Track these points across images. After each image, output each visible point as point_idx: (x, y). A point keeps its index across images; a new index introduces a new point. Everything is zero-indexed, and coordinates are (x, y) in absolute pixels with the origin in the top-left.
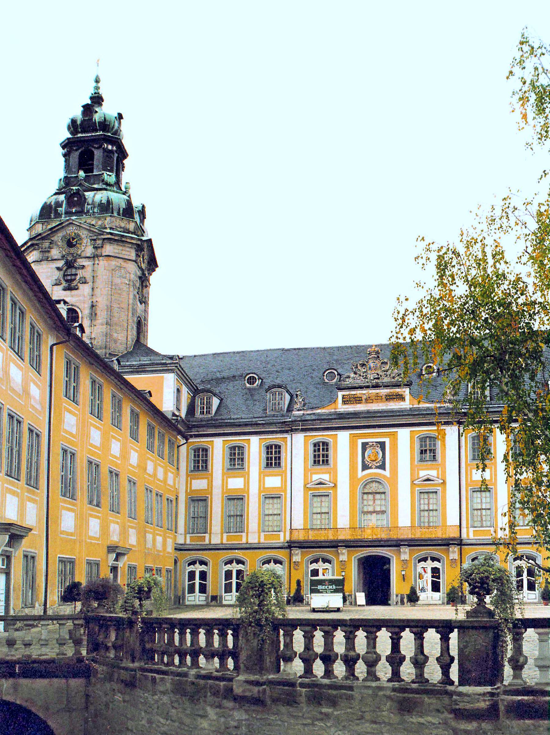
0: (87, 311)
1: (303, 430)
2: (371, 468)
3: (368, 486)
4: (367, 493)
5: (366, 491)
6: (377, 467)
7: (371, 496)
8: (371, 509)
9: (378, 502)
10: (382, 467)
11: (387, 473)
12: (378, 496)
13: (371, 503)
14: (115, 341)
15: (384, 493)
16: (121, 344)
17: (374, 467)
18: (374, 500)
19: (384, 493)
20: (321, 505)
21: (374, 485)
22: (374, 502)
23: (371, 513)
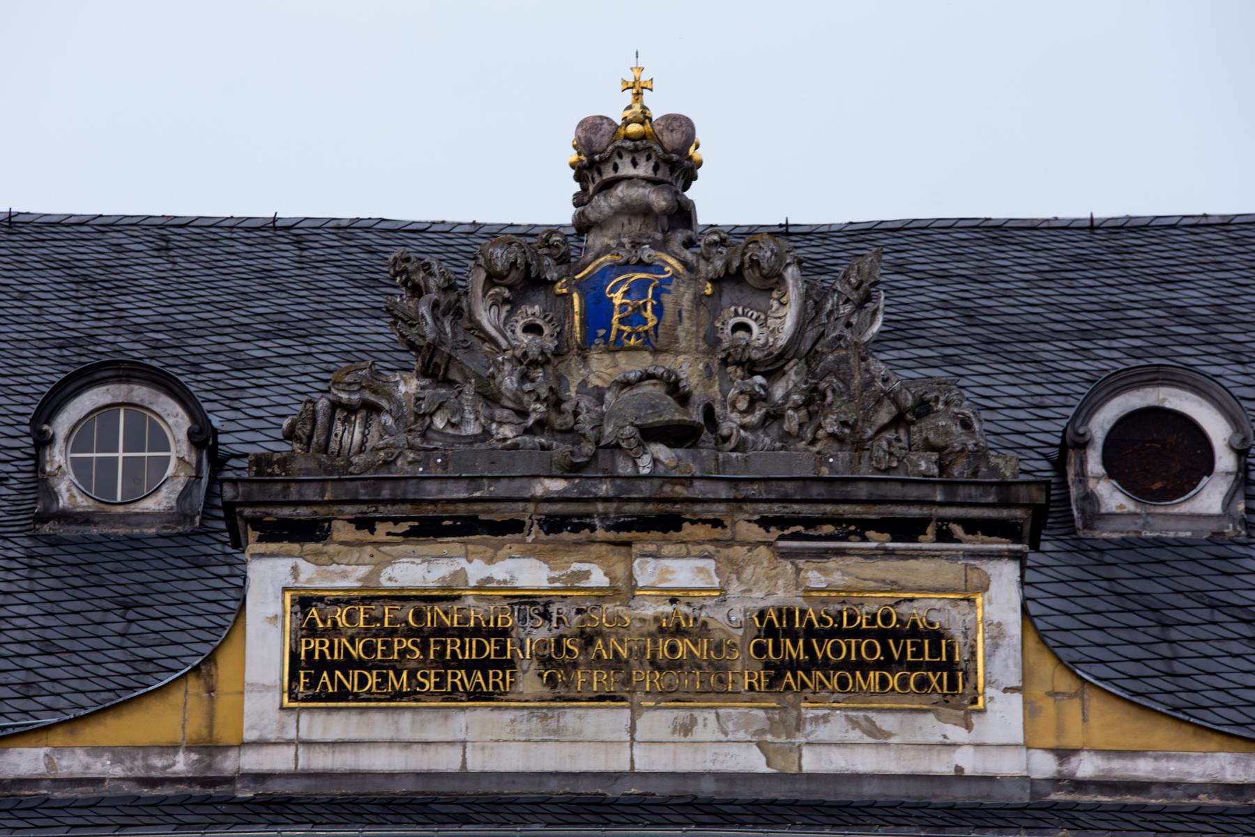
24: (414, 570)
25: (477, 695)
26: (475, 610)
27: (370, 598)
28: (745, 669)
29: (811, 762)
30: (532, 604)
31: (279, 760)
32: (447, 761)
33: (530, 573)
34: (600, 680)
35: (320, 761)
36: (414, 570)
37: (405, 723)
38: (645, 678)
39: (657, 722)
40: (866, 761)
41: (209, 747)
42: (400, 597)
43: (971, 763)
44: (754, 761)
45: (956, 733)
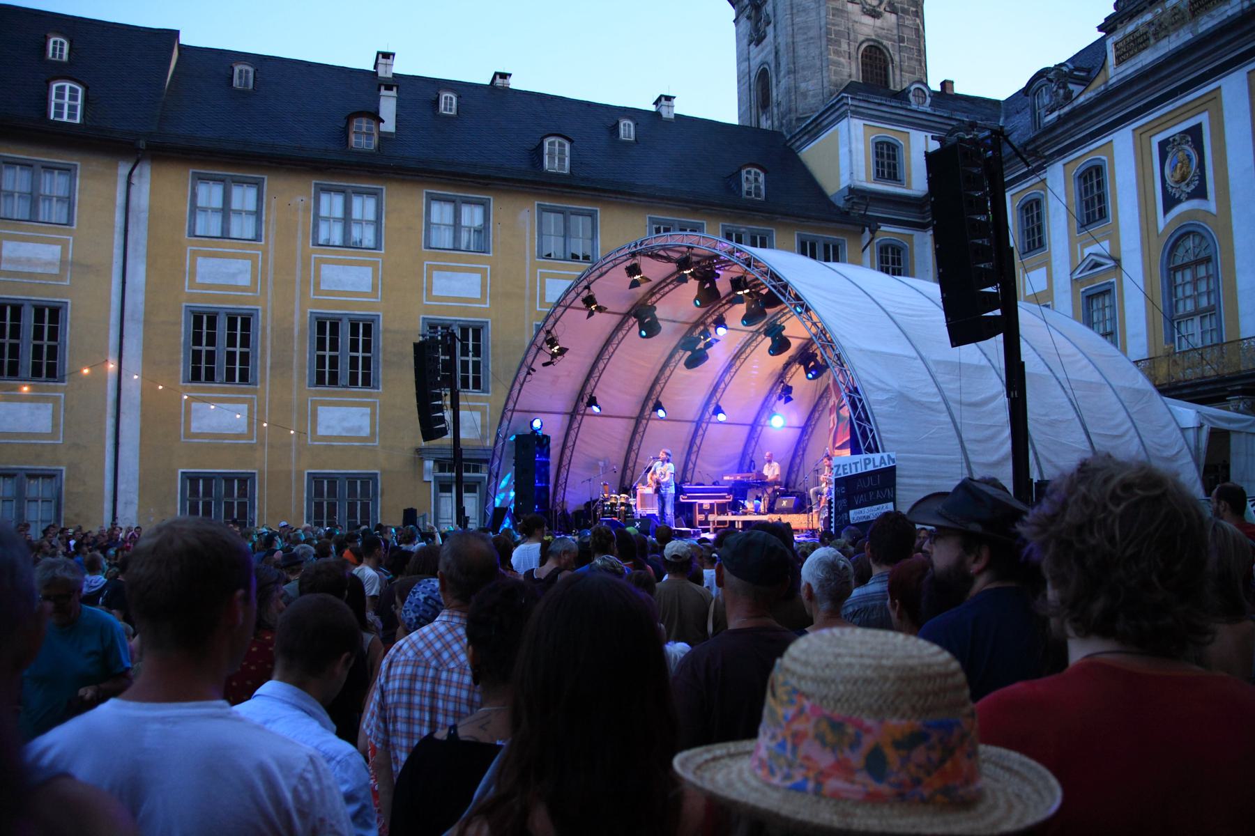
0: (773, 66)
1: (1061, 153)
2: (1179, 201)
3: (1180, 252)
4: (1183, 267)
5: (1178, 262)
6: (1191, 196)
7: (1188, 275)
8: (1190, 306)
9: (1203, 287)
10: (1200, 193)
11: (1211, 205)
12: (1202, 271)
13: (1189, 290)
14: (805, 95)
15: (1207, 260)
16: (814, 96)
17: (1184, 196)
18: (1195, 282)
19: (1207, 260)
20: (1104, 315)
21: (1190, 243)
22: (1195, 288)
23: (1190, 316)
24: (1130, 28)
25: (1144, 48)
26: (1142, 30)
27: (1125, 37)
28: (1188, 15)
29: (1200, 31)
30: (1150, 24)
31: (1114, 80)
32: (1139, 66)
33: (1148, 17)
34: (1163, 33)
35: (1121, 76)
36: (1130, 28)
37: (1133, 61)
38: (1171, 28)
39: (1173, 37)
40: (1210, 25)
41: (1106, 82)
42: (1130, 35)
43: (1230, 13)
44: (1190, 36)
45: (1227, 7)
